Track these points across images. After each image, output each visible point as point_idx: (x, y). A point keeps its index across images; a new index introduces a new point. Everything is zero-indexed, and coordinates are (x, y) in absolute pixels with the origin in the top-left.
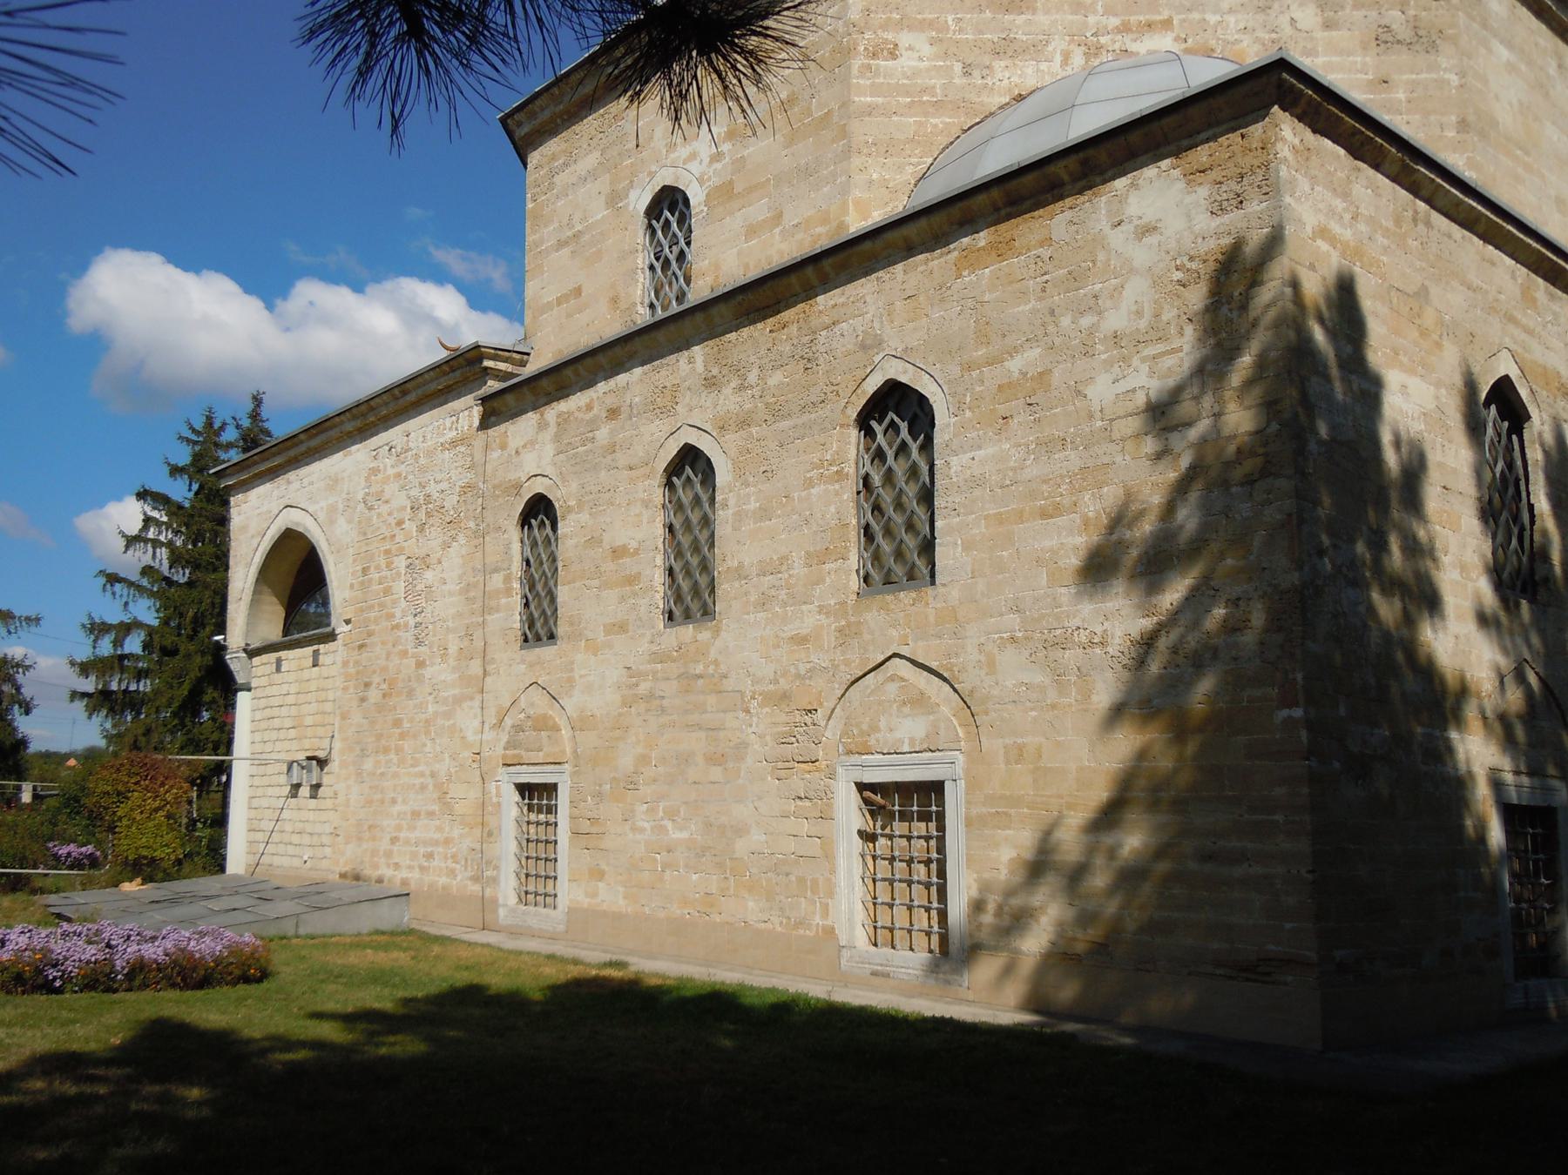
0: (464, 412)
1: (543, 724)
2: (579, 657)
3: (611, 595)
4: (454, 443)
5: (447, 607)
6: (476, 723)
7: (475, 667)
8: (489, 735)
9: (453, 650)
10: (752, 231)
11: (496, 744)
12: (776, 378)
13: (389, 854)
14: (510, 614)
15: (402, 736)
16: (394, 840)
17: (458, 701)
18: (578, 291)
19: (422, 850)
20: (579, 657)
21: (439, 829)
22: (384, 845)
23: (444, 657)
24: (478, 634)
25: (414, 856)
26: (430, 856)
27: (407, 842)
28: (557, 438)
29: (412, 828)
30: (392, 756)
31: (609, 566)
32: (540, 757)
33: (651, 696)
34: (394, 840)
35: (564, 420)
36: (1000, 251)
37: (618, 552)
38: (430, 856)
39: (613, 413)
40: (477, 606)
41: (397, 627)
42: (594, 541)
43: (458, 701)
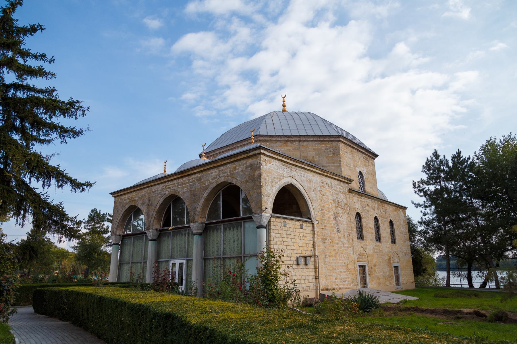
1: (363, 254)
2: (367, 244)
5: (344, 226)
6: (352, 252)
7: (351, 240)
8: (355, 255)
9: (346, 236)
10: (371, 188)
11: (356, 257)
13: (335, 282)
14: (355, 232)
15: (336, 253)
16: (336, 279)
17: (348, 247)
19: (343, 280)
21: (346, 275)
22: (334, 280)
23: (344, 238)
24: (351, 234)
25: (341, 282)
26: (345, 281)
27: (339, 279)
28: (361, 204)
29: (341, 275)
30: (334, 258)
32: (363, 260)
33: (376, 252)
34: (336, 279)
35: (361, 202)
37: (370, 228)
38: (345, 281)
39: (368, 205)
40: (350, 228)
41: (332, 227)
42: (367, 225)
43: (348, 247)
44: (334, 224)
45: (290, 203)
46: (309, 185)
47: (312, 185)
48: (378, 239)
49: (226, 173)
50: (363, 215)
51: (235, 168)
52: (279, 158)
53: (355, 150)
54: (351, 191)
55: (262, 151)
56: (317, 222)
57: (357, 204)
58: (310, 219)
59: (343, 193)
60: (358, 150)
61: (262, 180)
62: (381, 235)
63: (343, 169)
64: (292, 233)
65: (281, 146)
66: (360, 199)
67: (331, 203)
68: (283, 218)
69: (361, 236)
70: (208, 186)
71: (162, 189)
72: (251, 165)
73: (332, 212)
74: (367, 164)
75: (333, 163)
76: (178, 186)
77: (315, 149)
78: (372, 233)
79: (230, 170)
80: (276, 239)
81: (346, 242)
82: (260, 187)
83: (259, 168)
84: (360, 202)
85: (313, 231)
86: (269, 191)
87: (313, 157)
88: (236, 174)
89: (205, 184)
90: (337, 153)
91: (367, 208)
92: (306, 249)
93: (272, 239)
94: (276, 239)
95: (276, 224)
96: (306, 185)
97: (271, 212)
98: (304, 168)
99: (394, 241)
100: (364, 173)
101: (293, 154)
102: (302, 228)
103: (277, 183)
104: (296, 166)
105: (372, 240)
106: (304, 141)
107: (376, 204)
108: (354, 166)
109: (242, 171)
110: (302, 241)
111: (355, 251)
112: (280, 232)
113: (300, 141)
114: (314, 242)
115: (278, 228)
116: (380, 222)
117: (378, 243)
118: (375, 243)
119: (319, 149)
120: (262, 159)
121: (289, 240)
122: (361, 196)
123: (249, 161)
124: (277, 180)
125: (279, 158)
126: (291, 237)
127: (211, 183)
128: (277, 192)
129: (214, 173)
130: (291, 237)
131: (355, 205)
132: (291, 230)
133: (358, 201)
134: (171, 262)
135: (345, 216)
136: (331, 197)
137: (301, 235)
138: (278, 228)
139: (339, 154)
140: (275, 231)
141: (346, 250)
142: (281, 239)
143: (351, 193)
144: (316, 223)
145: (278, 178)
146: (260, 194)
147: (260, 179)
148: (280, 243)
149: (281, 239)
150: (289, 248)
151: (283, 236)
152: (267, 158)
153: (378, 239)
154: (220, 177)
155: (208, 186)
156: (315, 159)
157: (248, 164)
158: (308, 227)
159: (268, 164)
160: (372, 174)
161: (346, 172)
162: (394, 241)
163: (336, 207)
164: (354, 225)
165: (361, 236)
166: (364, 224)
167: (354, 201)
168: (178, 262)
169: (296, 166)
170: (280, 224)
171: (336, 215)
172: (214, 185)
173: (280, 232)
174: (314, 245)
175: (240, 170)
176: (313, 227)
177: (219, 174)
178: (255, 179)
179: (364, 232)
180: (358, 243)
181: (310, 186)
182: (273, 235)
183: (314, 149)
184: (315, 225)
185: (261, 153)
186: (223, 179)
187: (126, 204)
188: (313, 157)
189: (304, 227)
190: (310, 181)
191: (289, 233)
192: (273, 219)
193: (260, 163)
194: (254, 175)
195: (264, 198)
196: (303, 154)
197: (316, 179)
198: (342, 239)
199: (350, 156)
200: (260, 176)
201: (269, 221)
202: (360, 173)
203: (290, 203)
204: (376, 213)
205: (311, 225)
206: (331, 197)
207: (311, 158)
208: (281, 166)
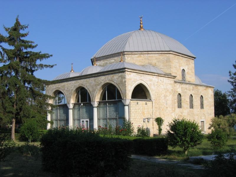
0: (171, 81)
3: (186, 105)
4: (170, 84)
5: (169, 102)
7: (174, 109)
10: (190, 78)
12: (197, 92)
14: (176, 105)
18: (176, 73)
20: (184, 110)
28: (181, 88)
31: (186, 102)
35: (182, 88)
36: (206, 90)
37: (187, 101)
39: (186, 89)
42: (185, 100)
43: (172, 113)
44: (164, 101)
45: (141, 92)
46: (150, 83)
47: (152, 82)
48: (192, 106)
49: (109, 78)
50: (181, 94)
51: (113, 76)
52: (135, 71)
53: (180, 57)
54: (175, 82)
55: (126, 70)
56: (154, 101)
57: (179, 88)
58: (150, 99)
59: (170, 84)
60: (182, 56)
61: (126, 84)
62: (194, 105)
63: (172, 69)
64: (141, 107)
65: (138, 57)
66: (181, 86)
67: (163, 90)
68: (137, 100)
69: (180, 106)
70: (100, 84)
71: (75, 83)
72: (121, 76)
73: (163, 95)
74: (188, 64)
75: (167, 66)
76: (83, 82)
77: (156, 59)
78: (188, 104)
79: (111, 77)
80: (133, 111)
81: (171, 110)
82: (126, 87)
83: (125, 78)
84: (181, 88)
85: (152, 105)
86: (130, 88)
87: (155, 63)
88: (114, 79)
89: (98, 83)
90: (168, 61)
91: (185, 90)
92: (148, 114)
93: (131, 111)
94: (133, 111)
95: (133, 103)
96: (149, 83)
97: (131, 98)
98: (148, 74)
99: (202, 106)
100: (185, 70)
101: (144, 62)
102: (146, 104)
103: (133, 84)
104: (144, 74)
105: (187, 108)
106: (150, 54)
107: (191, 87)
108: (179, 66)
109: (117, 78)
110: (146, 111)
111: (176, 114)
112: (135, 107)
113: (148, 54)
114: (153, 111)
115: (134, 105)
116: (193, 97)
117: (191, 109)
118: (189, 109)
119: (159, 58)
120: (126, 73)
121: (139, 111)
122: (182, 84)
123: (120, 74)
124: (133, 83)
125: (135, 71)
126: (141, 109)
127: (101, 83)
128: (134, 88)
129: (103, 78)
130: (141, 109)
131: (178, 90)
132: (141, 106)
133: (180, 87)
134: (81, 120)
135: (171, 96)
136: (162, 87)
137: (146, 108)
138: (134, 105)
139: (170, 61)
140: (133, 107)
141: (171, 114)
142: (135, 110)
143: (175, 83)
144: (154, 101)
145: (134, 82)
146: (126, 90)
147: (125, 83)
148: (135, 112)
149: (135, 110)
150: (139, 114)
151: (136, 109)
152: (129, 73)
153: (192, 106)
154: (106, 80)
155: (100, 84)
156: (156, 64)
157: (120, 75)
158: (149, 103)
159: (129, 75)
160: (191, 69)
161: (174, 72)
162: (202, 106)
163: (166, 92)
164: (176, 101)
165: (180, 106)
166: (183, 100)
167: (177, 87)
168: (85, 120)
169: (144, 74)
170: (135, 104)
171: (165, 96)
172: (103, 84)
173: (135, 107)
174: (153, 112)
175: (116, 77)
176: (152, 104)
177: (105, 79)
178: (124, 84)
179: (182, 104)
180: (178, 110)
181: (150, 83)
182: (131, 109)
183: (156, 58)
184: (153, 103)
185: (126, 71)
186: (107, 81)
187: (53, 89)
188: (155, 63)
189: (147, 104)
190: (151, 80)
191: (139, 107)
192: (132, 102)
193: (125, 75)
194: (123, 81)
195: (127, 92)
196: (150, 62)
197: (155, 79)
198: (168, 109)
199: (177, 61)
200: (125, 82)
201: (130, 102)
202: (183, 70)
203: (141, 92)
204: (192, 92)
205: (151, 103)
206: (162, 87)
207: (154, 64)
208: (136, 75)
